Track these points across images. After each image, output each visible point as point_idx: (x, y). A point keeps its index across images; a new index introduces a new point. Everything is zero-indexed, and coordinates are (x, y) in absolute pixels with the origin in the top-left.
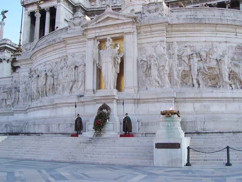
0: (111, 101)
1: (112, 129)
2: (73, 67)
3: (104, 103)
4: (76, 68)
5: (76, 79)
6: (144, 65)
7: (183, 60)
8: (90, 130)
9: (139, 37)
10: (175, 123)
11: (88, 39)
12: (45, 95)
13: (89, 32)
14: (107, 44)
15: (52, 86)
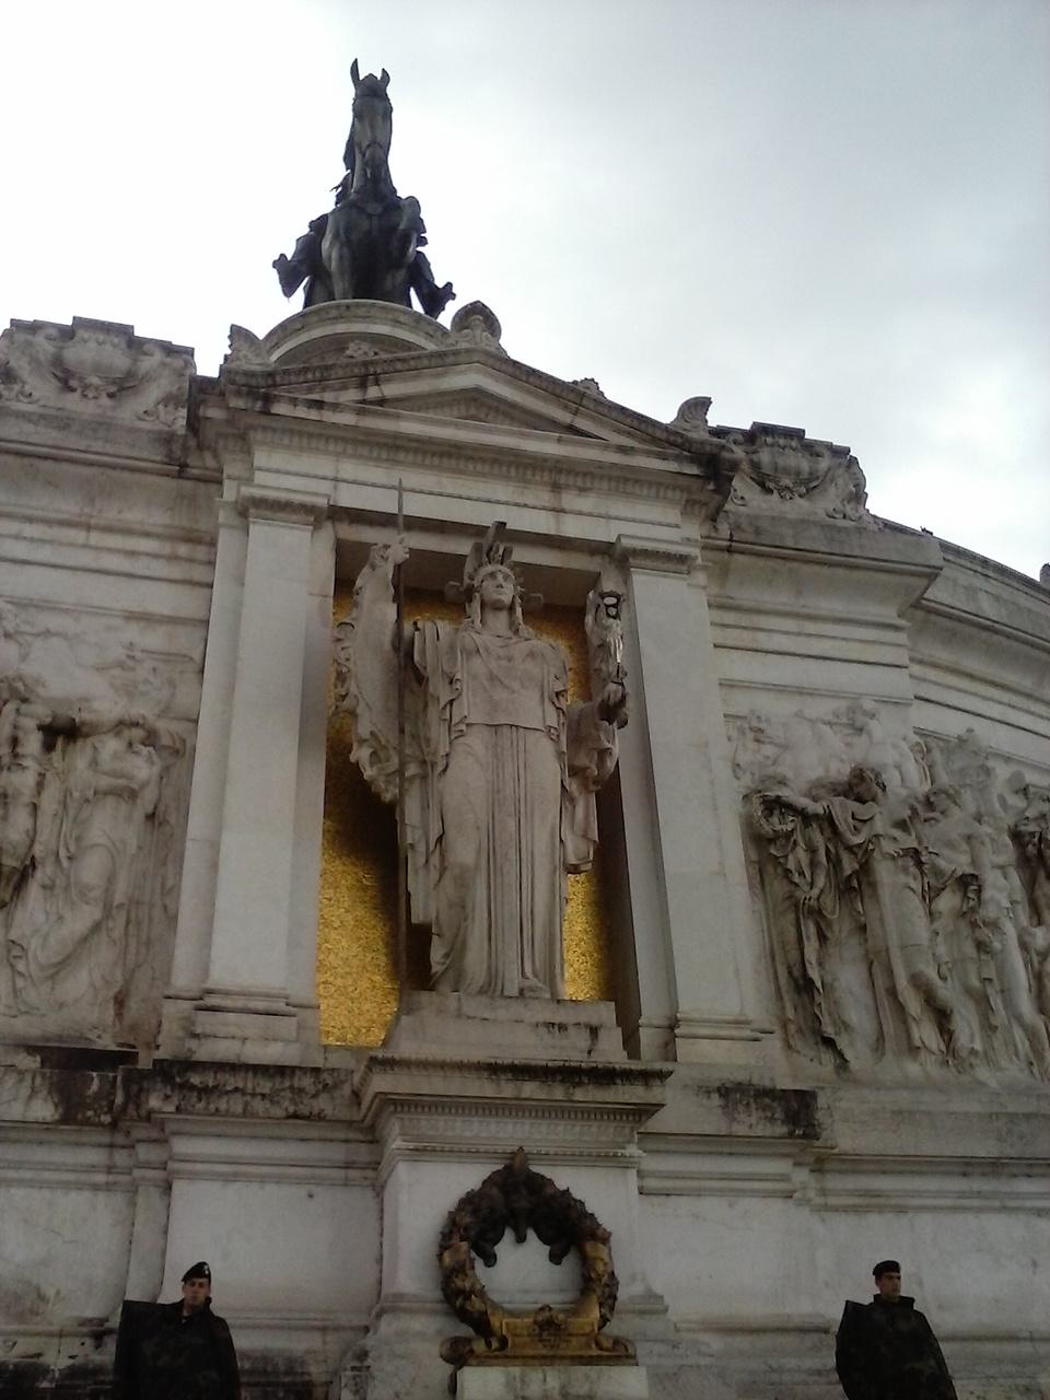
2: (29, 723)
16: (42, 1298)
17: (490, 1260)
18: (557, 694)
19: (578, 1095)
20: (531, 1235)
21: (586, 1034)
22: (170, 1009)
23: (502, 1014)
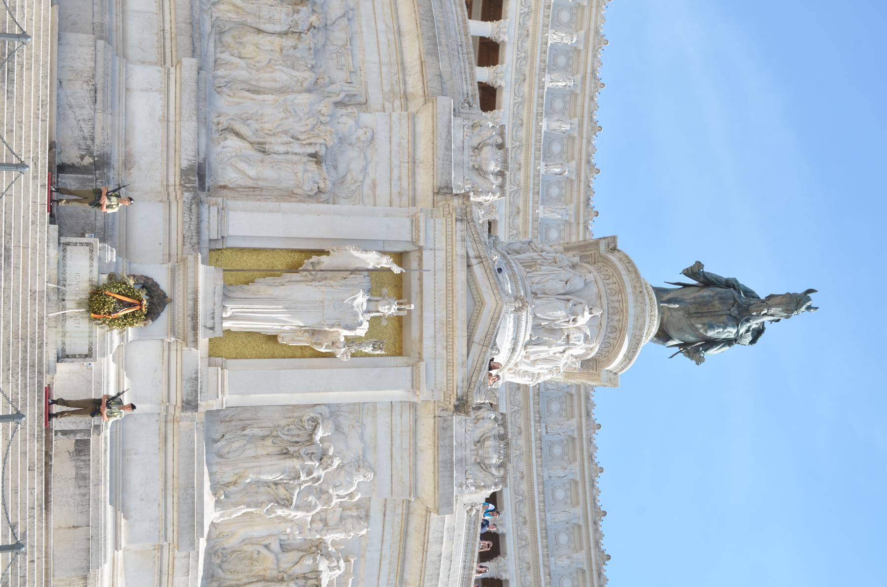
3: (171, 301)
7: (303, 556)
8: (68, 254)
9: (397, 408)
15: (254, 25)
16: (130, 169)
19: (189, 319)
22: (220, 200)
23: (217, 299)
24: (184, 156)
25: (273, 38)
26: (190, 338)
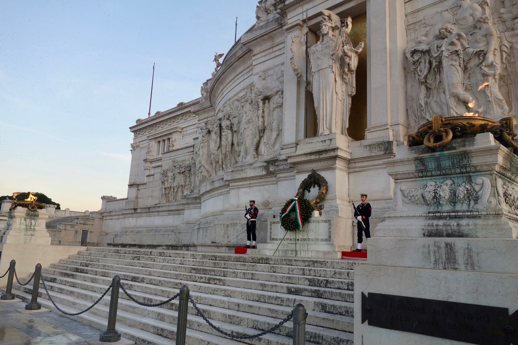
0: (330, 163)
1: (326, 238)
2: (260, 100)
4: (267, 102)
5: (265, 124)
6: (422, 65)
8: (275, 237)
10: (479, 180)
11: (288, 29)
12: (221, 168)
13: (289, 16)
14: (324, 27)
15: (230, 147)
17: (309, 191)
18: (332, 55)
20: (316, 186)
21: (329, 141)
24: (261, 174)
25: (234, 137)
26: (332, 154)
